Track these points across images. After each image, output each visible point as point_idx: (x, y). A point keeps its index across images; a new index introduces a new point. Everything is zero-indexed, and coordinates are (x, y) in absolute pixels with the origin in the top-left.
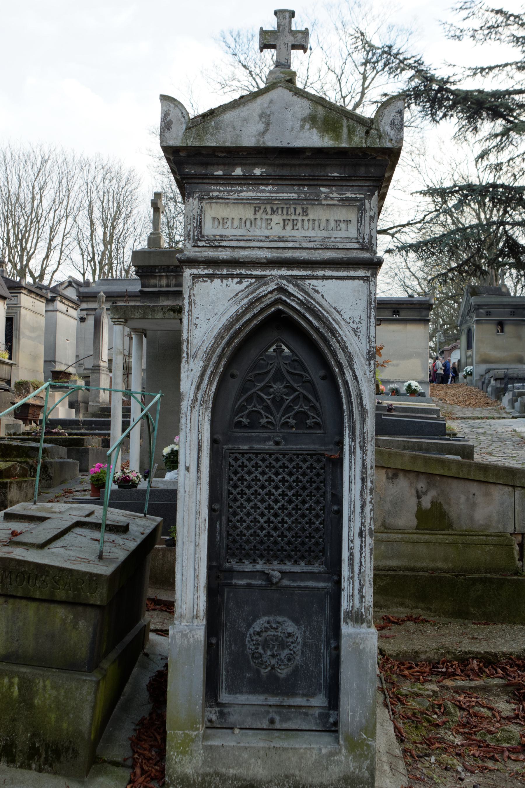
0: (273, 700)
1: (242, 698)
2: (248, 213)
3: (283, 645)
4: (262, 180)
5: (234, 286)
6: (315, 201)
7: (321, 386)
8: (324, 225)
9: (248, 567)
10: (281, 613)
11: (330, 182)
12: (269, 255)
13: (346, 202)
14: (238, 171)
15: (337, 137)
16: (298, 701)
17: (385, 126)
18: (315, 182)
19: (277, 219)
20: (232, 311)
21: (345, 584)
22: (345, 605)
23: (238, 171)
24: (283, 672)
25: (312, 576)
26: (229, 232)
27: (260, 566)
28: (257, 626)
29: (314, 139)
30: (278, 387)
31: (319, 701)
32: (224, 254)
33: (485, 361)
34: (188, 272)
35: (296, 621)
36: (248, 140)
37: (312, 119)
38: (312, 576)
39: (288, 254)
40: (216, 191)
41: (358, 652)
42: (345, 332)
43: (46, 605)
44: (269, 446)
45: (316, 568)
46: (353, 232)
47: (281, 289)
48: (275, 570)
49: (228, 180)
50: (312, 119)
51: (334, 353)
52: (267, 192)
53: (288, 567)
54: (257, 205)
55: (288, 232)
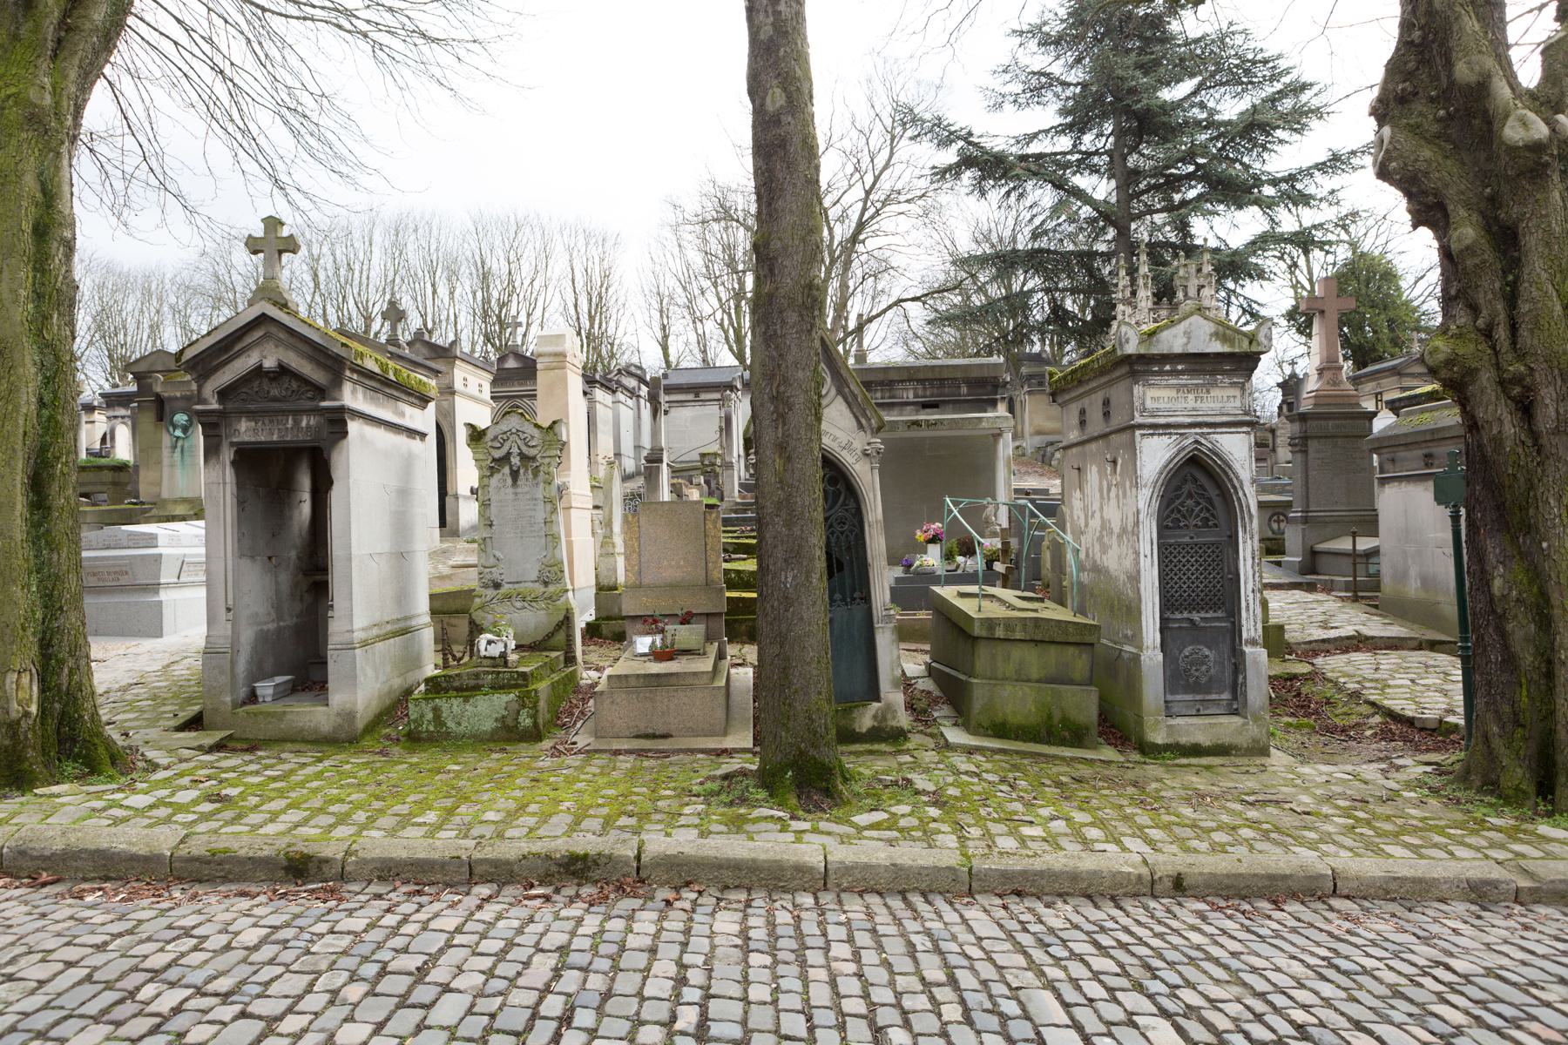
0: (1198, 697)
1: (1179, 697)
2: (1172, 393)
3: (1203, 663)
4: (1182, 372)
5: (1165, 439)
6: (1214, 385)
7: (1217, 501)
8: (1220, 400)
9: (1179, 616)
10: (1200, 643)
11: (1223, 373)
12: (1189, 420)
13: (1233, 385)
14: (1168, 368)
15: (1232, 345)
16: (1214, 697)
17: (1261, 337)
18: (1213, 373)
19: (1191, 396)
20: (1167, 456)
21: (1244, 622)
22: (1245, 636)
23: (1168, 368)
24: (1204, 680)
25: (1217, 619)
26: (1162, 406)
27: (1186, 615)
28: (1187, 652)
29: (1217, 347)
30: (1190, 502)
31: (1226, 696)
32: (1162, 421)
33: (1039, 433)
34: (1138, 433)
35: (1210, 648)
36: (1178, 349)
37: (1216, 335)
38: (1217, 619)
39: (1200, 419)
40: (1153, 380)
41: (1256, 662)
42: (1237, 466)
43: (1059, 648)
44: (1187, 539)
45: (1220, 614)
46: (1238, 404)
47: (1197, 442)
48: (1196, 616)
49: (1161, 373)
50: (1216, 335)
51: (1231, 480)
52: (1184, 380)
53: (1203, 615)
54: (1179, 388)
55: (1198, 405)
